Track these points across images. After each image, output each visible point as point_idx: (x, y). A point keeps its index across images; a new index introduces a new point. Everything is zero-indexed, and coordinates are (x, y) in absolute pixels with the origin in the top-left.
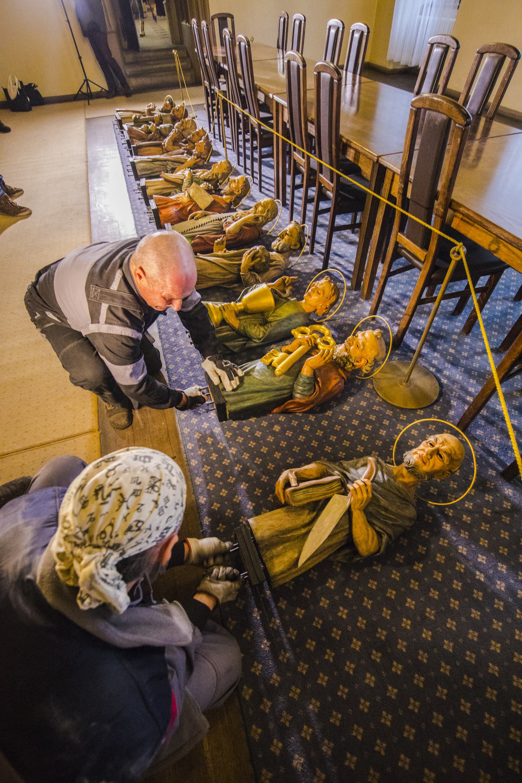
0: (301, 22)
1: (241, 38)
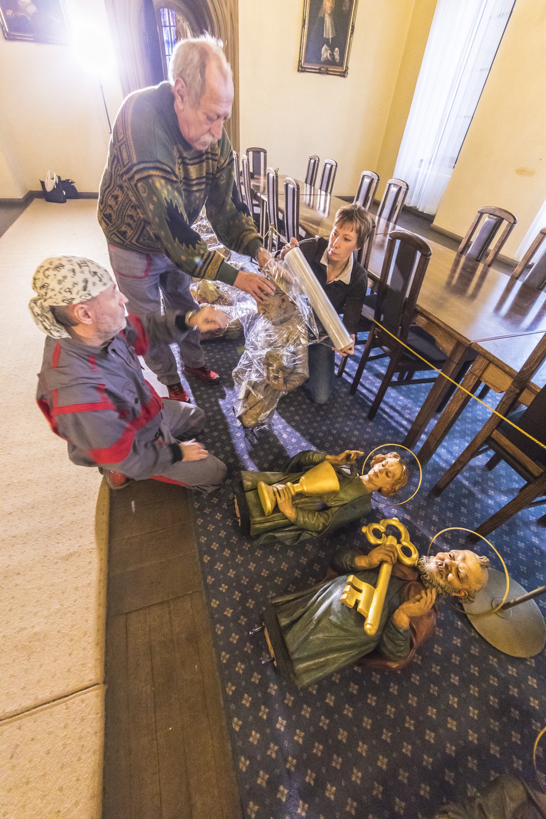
0: (332, 166)
1: (290, 181)
